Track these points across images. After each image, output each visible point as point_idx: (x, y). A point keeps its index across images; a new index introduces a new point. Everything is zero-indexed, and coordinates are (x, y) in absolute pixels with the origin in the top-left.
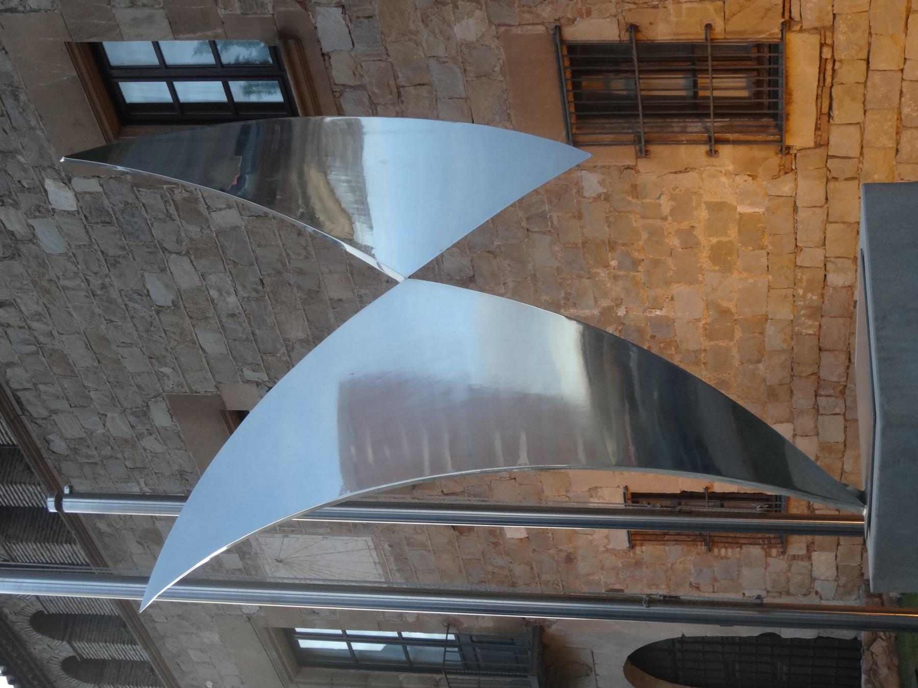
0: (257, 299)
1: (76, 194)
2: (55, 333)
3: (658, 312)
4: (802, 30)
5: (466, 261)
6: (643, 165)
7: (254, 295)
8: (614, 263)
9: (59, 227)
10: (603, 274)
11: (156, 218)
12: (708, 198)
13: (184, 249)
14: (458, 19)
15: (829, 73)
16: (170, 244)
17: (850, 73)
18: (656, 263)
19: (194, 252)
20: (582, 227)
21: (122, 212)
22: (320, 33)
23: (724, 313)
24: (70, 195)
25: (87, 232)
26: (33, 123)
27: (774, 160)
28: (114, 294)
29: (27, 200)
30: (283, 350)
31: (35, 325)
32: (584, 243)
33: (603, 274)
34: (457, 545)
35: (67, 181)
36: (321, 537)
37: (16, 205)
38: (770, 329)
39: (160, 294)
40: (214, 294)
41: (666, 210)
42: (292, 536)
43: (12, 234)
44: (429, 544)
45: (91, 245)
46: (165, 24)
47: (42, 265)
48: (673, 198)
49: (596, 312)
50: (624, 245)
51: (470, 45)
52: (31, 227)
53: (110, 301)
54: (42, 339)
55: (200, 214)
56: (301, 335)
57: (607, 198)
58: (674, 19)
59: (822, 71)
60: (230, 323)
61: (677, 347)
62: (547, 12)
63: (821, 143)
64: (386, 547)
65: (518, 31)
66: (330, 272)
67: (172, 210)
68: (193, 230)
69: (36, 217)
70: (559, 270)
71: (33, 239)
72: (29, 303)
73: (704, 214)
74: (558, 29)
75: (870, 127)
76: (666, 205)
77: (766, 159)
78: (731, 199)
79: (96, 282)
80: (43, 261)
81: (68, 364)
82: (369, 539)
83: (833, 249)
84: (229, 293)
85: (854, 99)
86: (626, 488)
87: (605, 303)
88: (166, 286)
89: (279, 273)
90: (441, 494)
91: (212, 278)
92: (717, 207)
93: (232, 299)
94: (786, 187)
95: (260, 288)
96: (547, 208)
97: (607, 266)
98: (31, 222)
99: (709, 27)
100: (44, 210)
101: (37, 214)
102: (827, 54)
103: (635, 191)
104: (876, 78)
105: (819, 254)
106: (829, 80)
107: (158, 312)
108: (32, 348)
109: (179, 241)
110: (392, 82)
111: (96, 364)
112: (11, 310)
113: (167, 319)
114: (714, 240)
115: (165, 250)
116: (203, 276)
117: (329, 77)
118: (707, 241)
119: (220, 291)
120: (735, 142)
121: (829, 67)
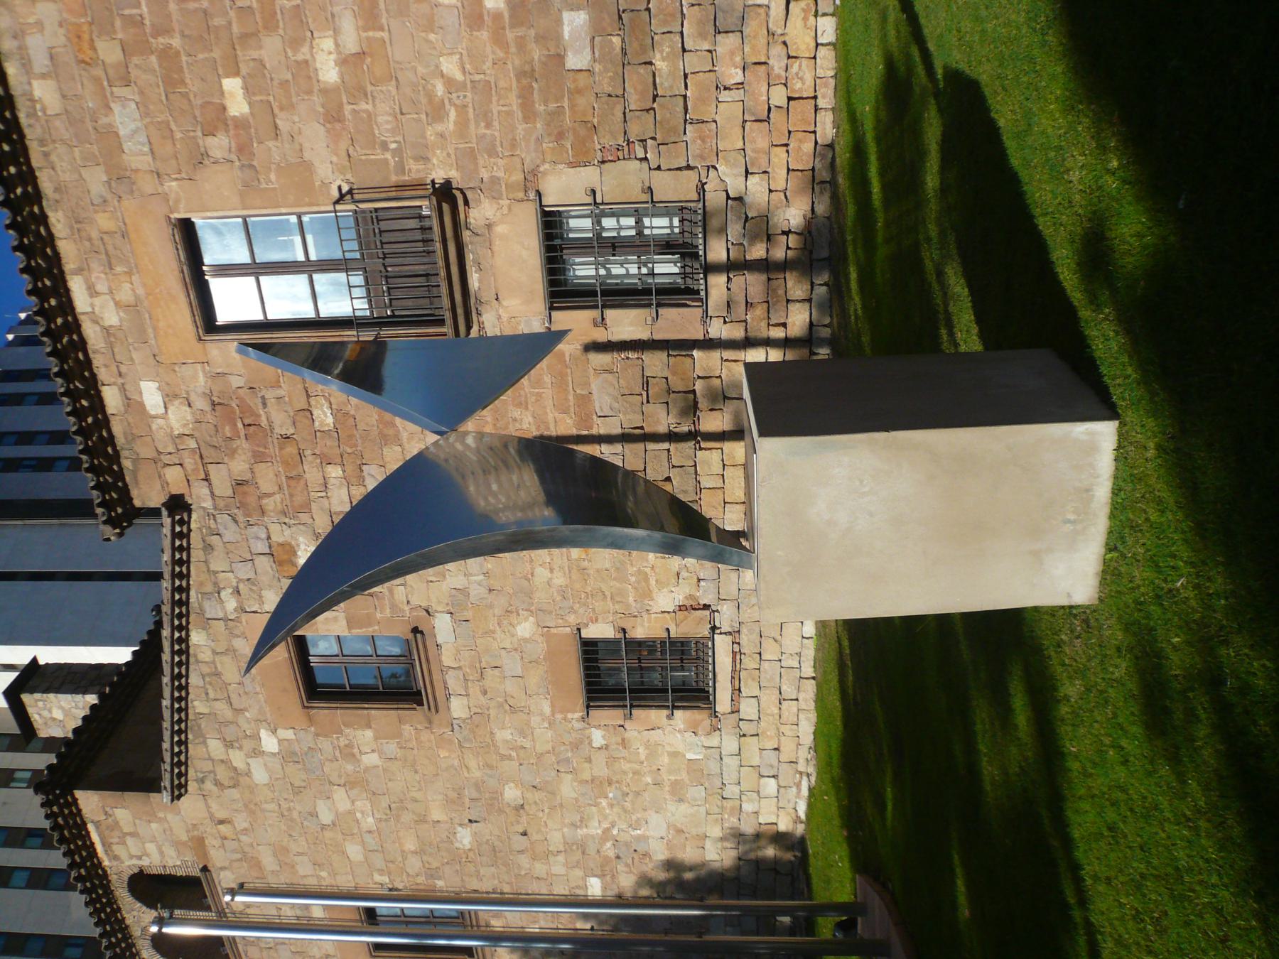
0: (386, 820)
1: (280, 741)
2: (255, 844)
3: (638, 832)
4: (721, 633)
5: (519, 793)
6: (628, 725)
7: (384, 817)
8: (611, 795)
9: (265, 765)
10: (604, 802)
11: (328, 760)
12: (668, 748)
13: (342, 782)
14: (519, 623)
15: (738, 661)
16: (334, 779)
17: (749, 663)
18: (638, 794)
19: (349, 784)
20: (591, 769)
21: (306, 754)
22: (436, 630)
23: (680, 831)
24: (275, 741)
26: (258, 689)
27: (707, 722)
28: (295, 815)
29: (248, 745)
30: (400, 859)
31: (243, 838)
32: (592, 780)
33: (604, 802)
35: (274, 731)
37: (240, 748)
38: (708, 844)
39: (326, 817)
40: (359, 815)
41: (643, 757)
43: (235, 769)
46: (344, 622)
47: (252, 792)
48: (647, 748)
49: (599, 831)
50: (617, 782)
51: (526, 640)
52: (248, 764)
53: (292, 820)
54: (247, 849)
55: (353, 755)
56: (413, 848)
57: (607, 747)
58: (646, 625)
59: (734, 661)
60: (368, 838)
61: (650, 858)
62: (572, 619)
63: (735, 711)
65: (554, 631)
66: (433, 801)
67: (337, 753)
68: (350, 767)
70: (577, 800)
71: (248, 774)
72: (241, 822)
73: (666, 760)
74: (579, 630)
75: (764, 699)
76: (643, 752)
77: (703, 720)
78: (681, 748)
79: (285, 805)
80: (252, 788)
81: (260, 868)
83: (744, 786)
84: (368, 815)
85: (753, 679)
87: (605, 825)
88: (330, 809)
89: (402, 801)
91: (358, 803)
92: (675, 755)
93: (370, 820)
94: (714, 741)
95: (388, 812)
96: (570, 754)
97: (606, 797)
98: (249, 760)
99: (668, 630)
100: (257, 752)
102: (736, 648)
103: (624, 743)
104: (765, 665)
105: (736, 789)
106: (738, 666)
107: (322, 829)
108: (239, 856)
109: (340, 776)
110: (478, 665)
111: (278, 868)
112: (229, 826)
113: (328, 834)
114: (673, 778)
115: (330, 782)
116: (353, 802)
117: (440, 661)
118: (667, 777)
119: (363, 813)
120: (684, 708)
121: (738, 657)
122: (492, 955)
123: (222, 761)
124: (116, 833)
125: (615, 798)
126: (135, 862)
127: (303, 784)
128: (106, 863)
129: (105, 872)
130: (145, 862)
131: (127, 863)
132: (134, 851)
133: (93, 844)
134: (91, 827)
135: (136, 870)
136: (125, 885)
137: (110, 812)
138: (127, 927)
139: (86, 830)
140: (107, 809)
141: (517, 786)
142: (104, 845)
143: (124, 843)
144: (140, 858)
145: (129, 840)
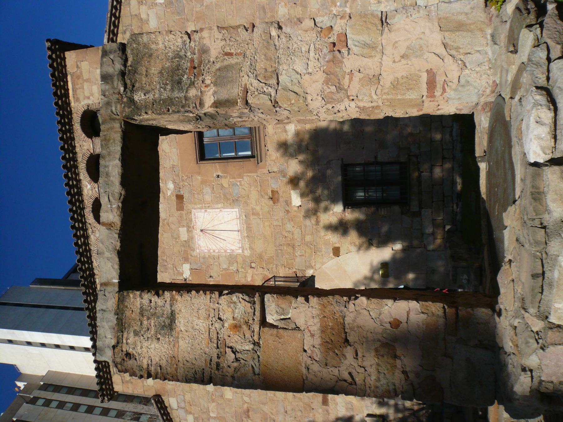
5: (286, 11)
8: (338, 4)
25: (165, 14)
34: (272, 214)
36: (219, 210)
37: (146, 4)
42: (208, 210)
43: (141, 19)
44: (261, 213)
45: (164, 22)
52: (148, 15)
64: (244, 216)
69: (151, 9)
82: (237, 210)
86: (342, 159)
90: (268, 172)
101: (151, 7)
122: (266, 154)
123: (136, 15)
124: (80, 81)
125: (341, 6)
126: (87, 102)
127: (174, 24)
128: (72, 104)
129: (71, 111)
130: (90, 102)
131: (82, 103)
132: (87, 94)
133: (68, 89)
134: (69, 78)
135: (86, 108)
136: (79, 121)
137: (79, 66)
138: (76, 153)
139: (67, 79)
140: (78, 63)
141: (286, 4)
142: (73, 90)
143: (83, 88)
144: (89, 98)
145: (86, 85)
